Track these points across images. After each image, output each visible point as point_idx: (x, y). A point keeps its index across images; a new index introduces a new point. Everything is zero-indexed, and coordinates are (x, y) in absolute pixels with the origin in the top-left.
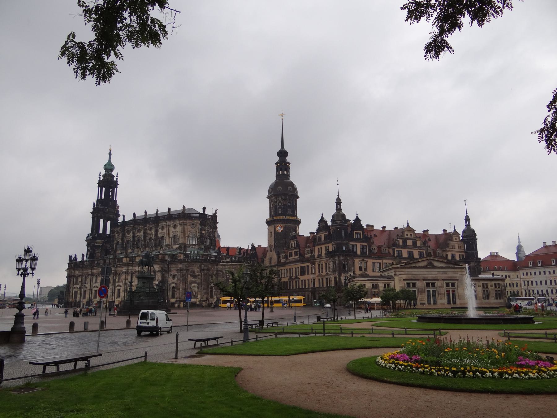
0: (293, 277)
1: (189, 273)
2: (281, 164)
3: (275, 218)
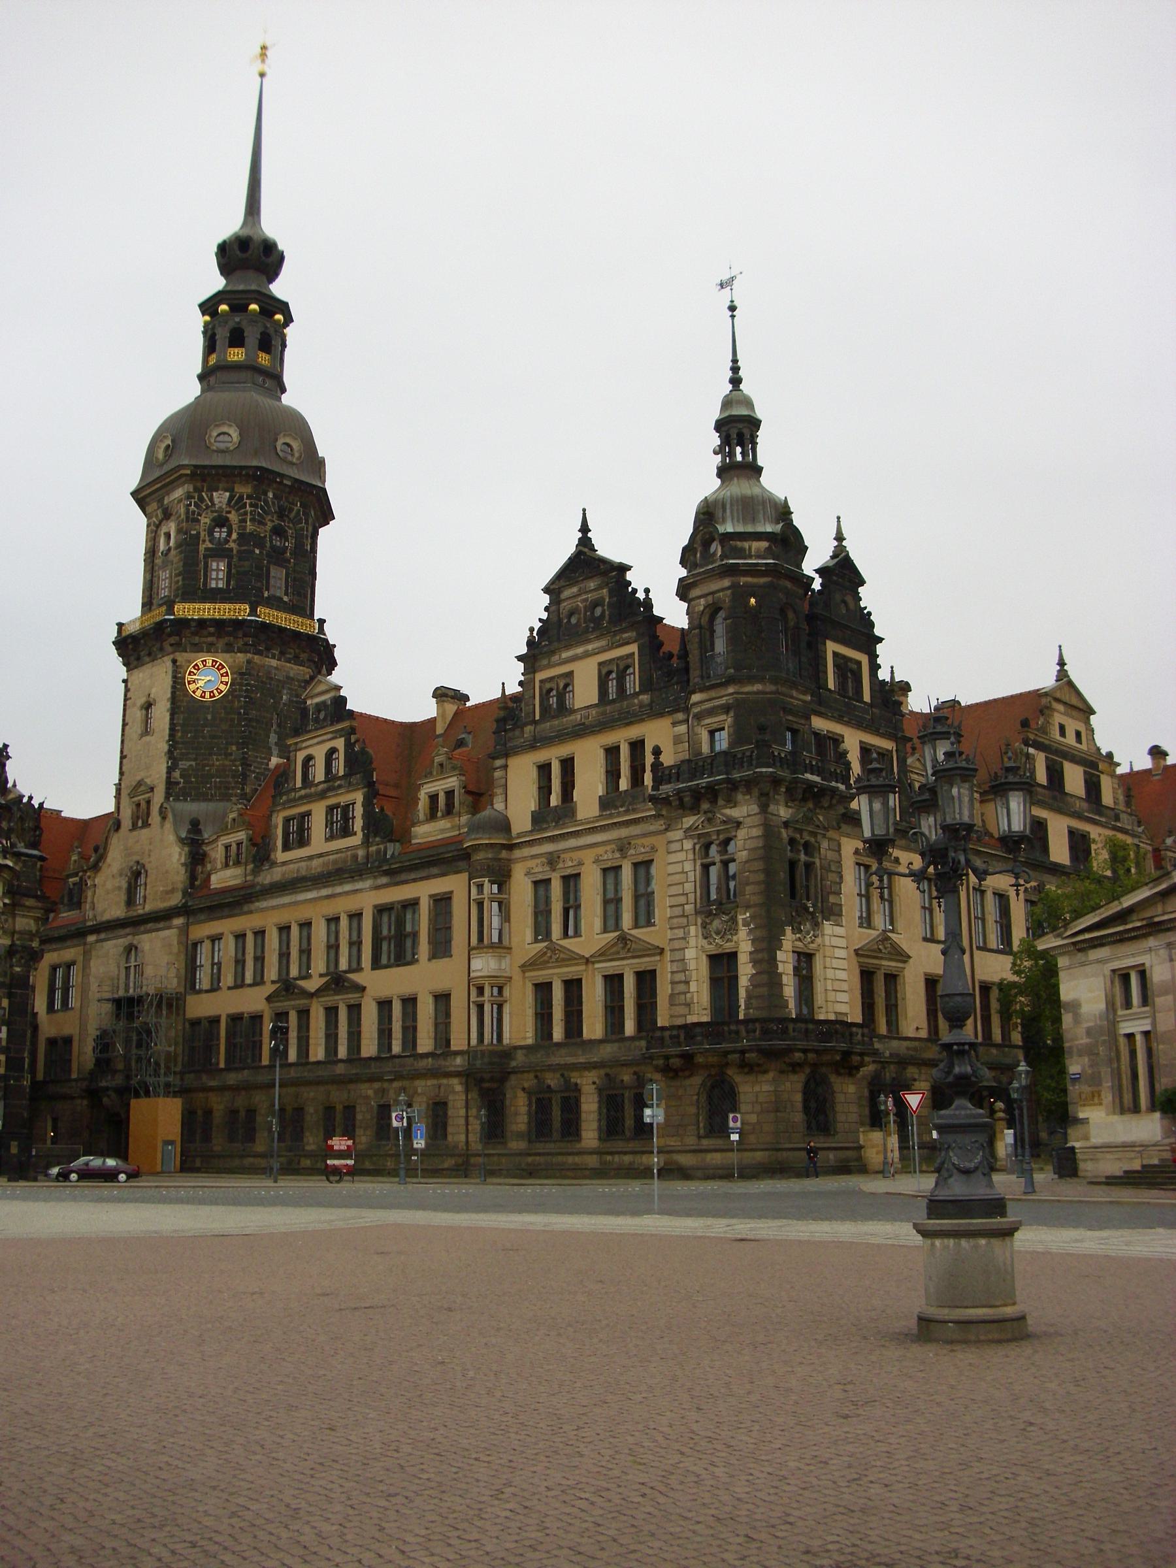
0: (312, 985)
2: (239, 308)
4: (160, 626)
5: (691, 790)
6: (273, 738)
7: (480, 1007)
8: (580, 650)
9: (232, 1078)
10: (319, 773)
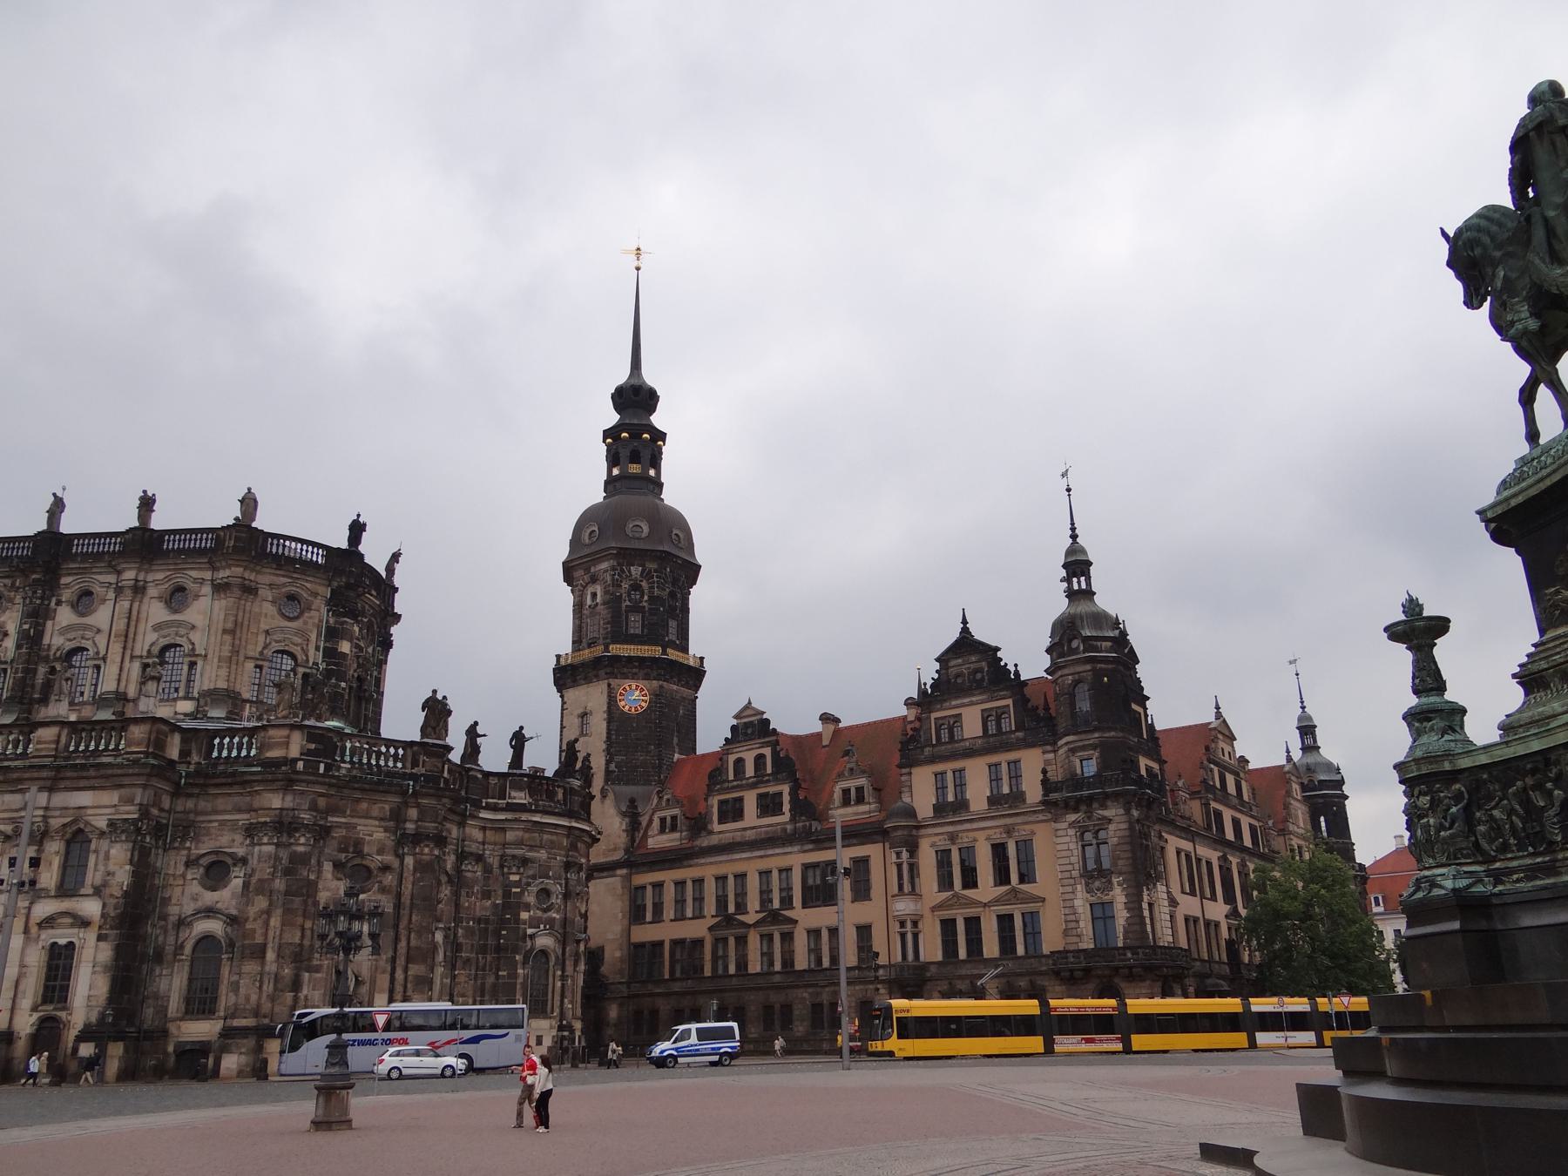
0: (751, 918)
1: (331, 849)
2: (636, 435)
3: (618, 649)
4: (597, 663)
5: (1063, 797)
6: (675, 740)
7: (903, 936)
8: (966, 700)
9: (677, 987)
10: (750, 771)
